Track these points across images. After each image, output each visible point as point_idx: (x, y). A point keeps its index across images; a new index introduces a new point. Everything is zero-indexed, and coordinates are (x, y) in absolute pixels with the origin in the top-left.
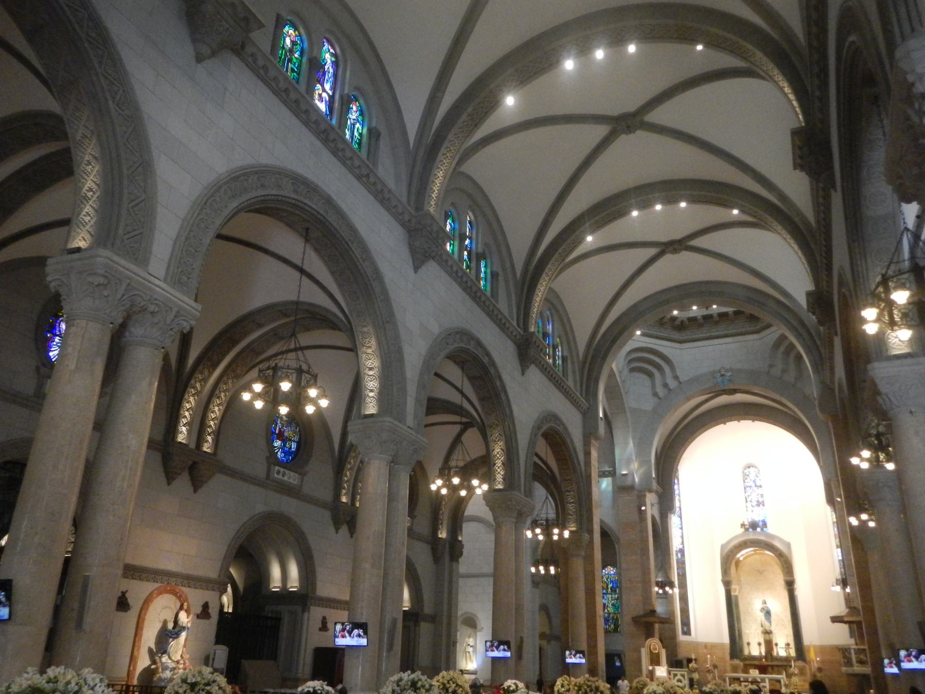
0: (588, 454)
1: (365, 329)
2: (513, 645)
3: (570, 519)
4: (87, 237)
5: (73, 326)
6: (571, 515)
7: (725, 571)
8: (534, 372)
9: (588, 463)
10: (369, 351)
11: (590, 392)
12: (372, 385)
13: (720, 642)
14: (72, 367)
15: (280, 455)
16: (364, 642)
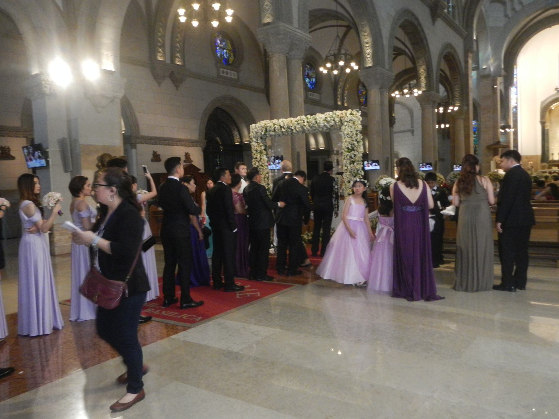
0: (466, 62)
1: (363, 23)
2: (433, 164)
3: (456, 99)
4: (270, 16)
5: (274, 57)
6: (457, 97)
7: (543, 116)
8: (440, 23)
9: (467, 68)
10: (366, 34)
11: (468, 25)
12: (368, 51)
13: (536, 154)
14: (278, 74)
15: (309, 85)
16: (378, 167)
